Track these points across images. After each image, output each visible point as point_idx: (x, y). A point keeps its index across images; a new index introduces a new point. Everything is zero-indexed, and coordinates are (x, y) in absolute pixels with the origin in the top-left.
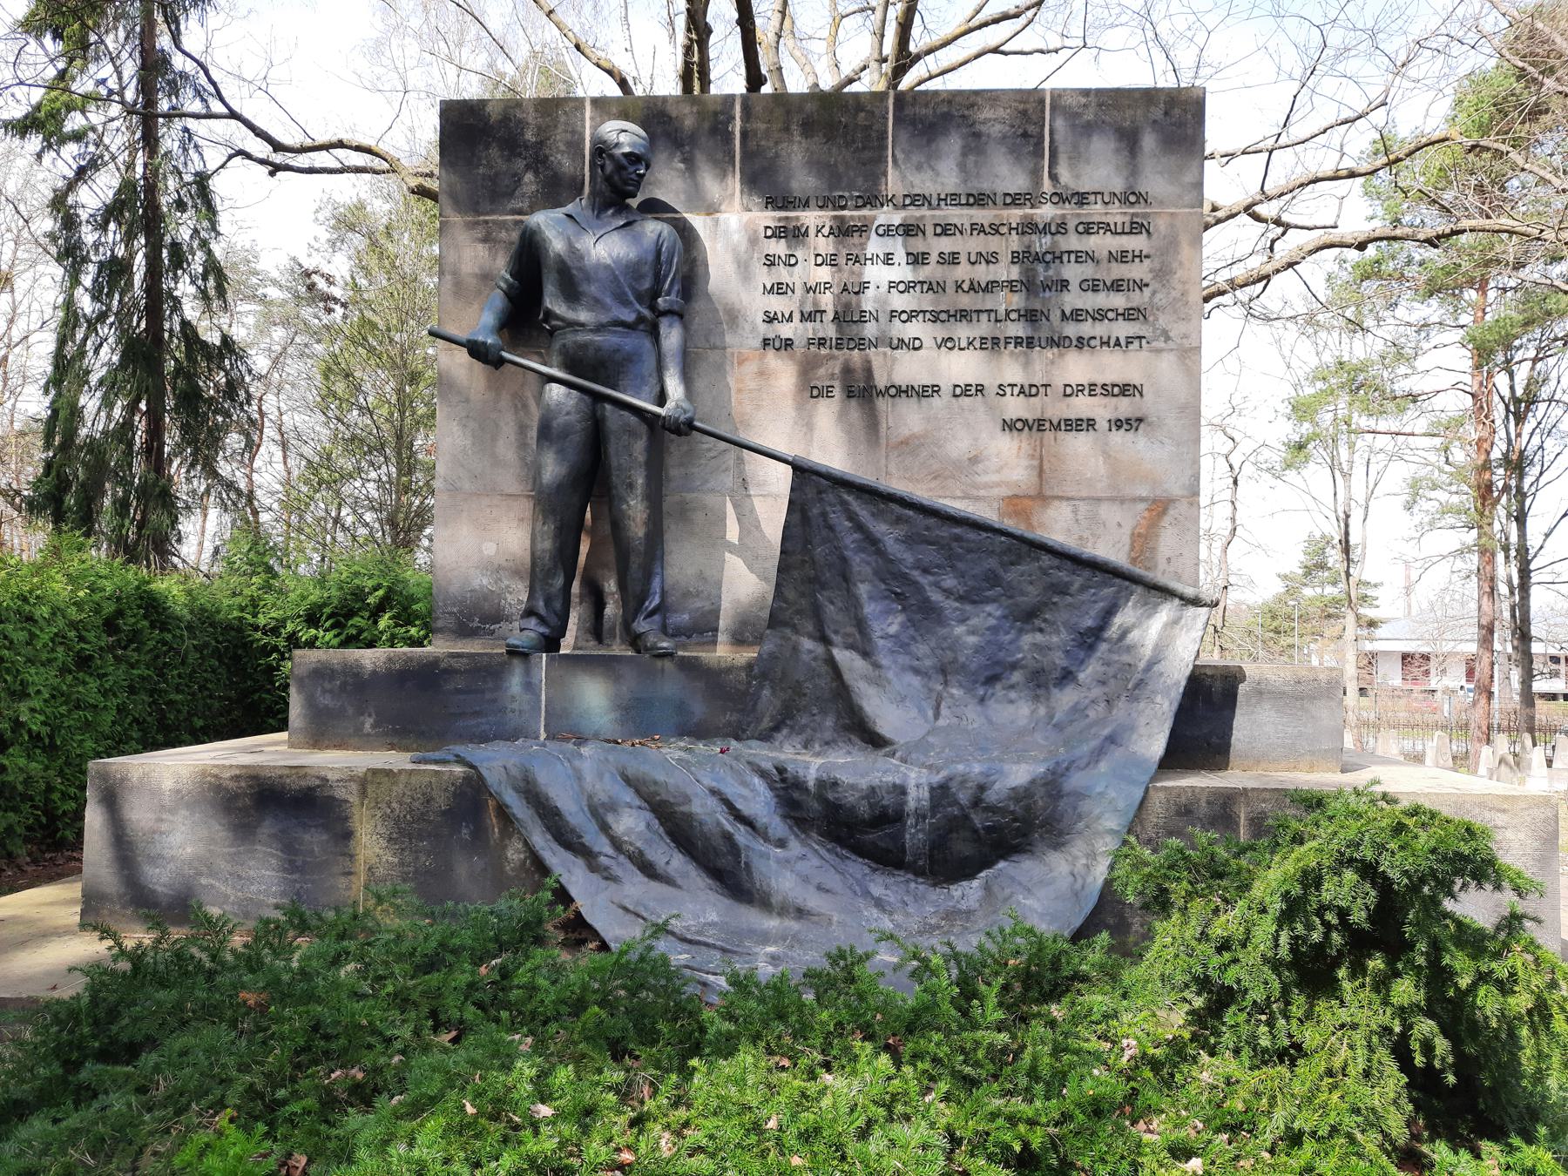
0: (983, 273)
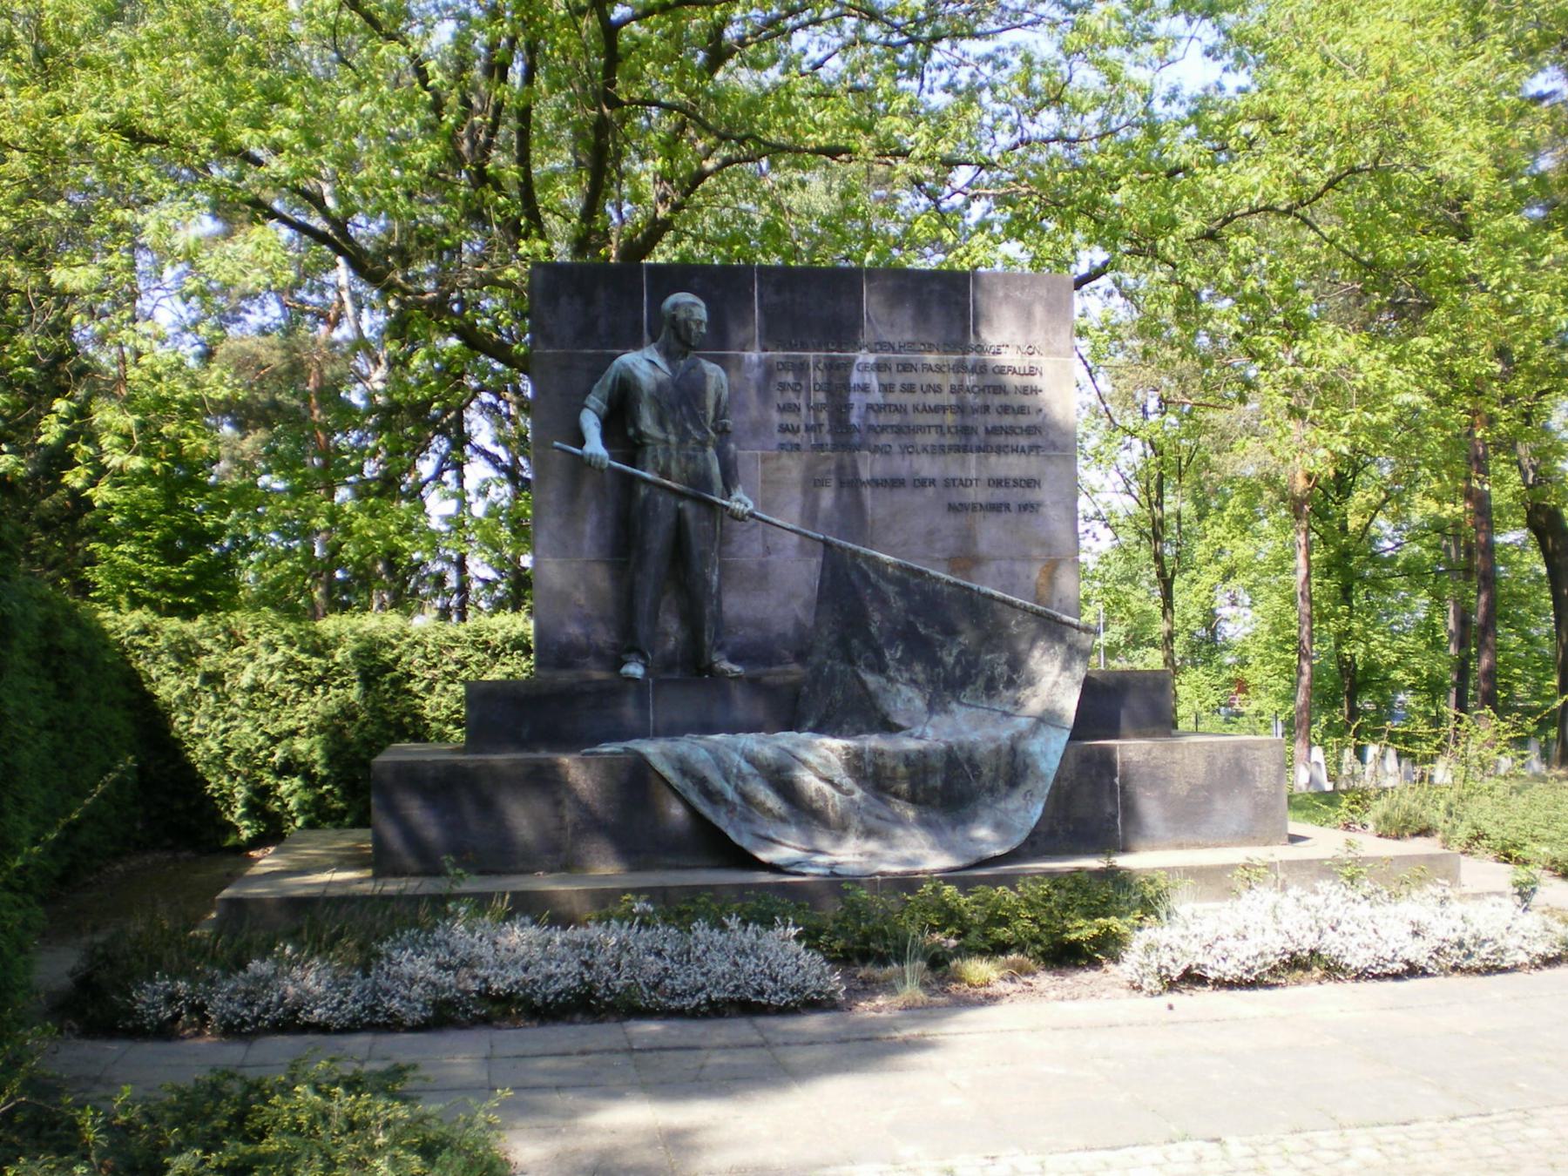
0: (932, 399)
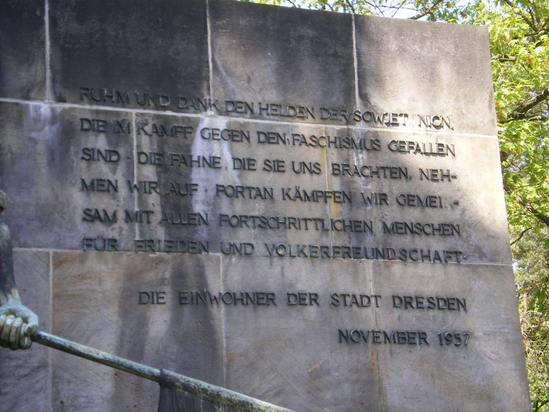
0: (308, 183)
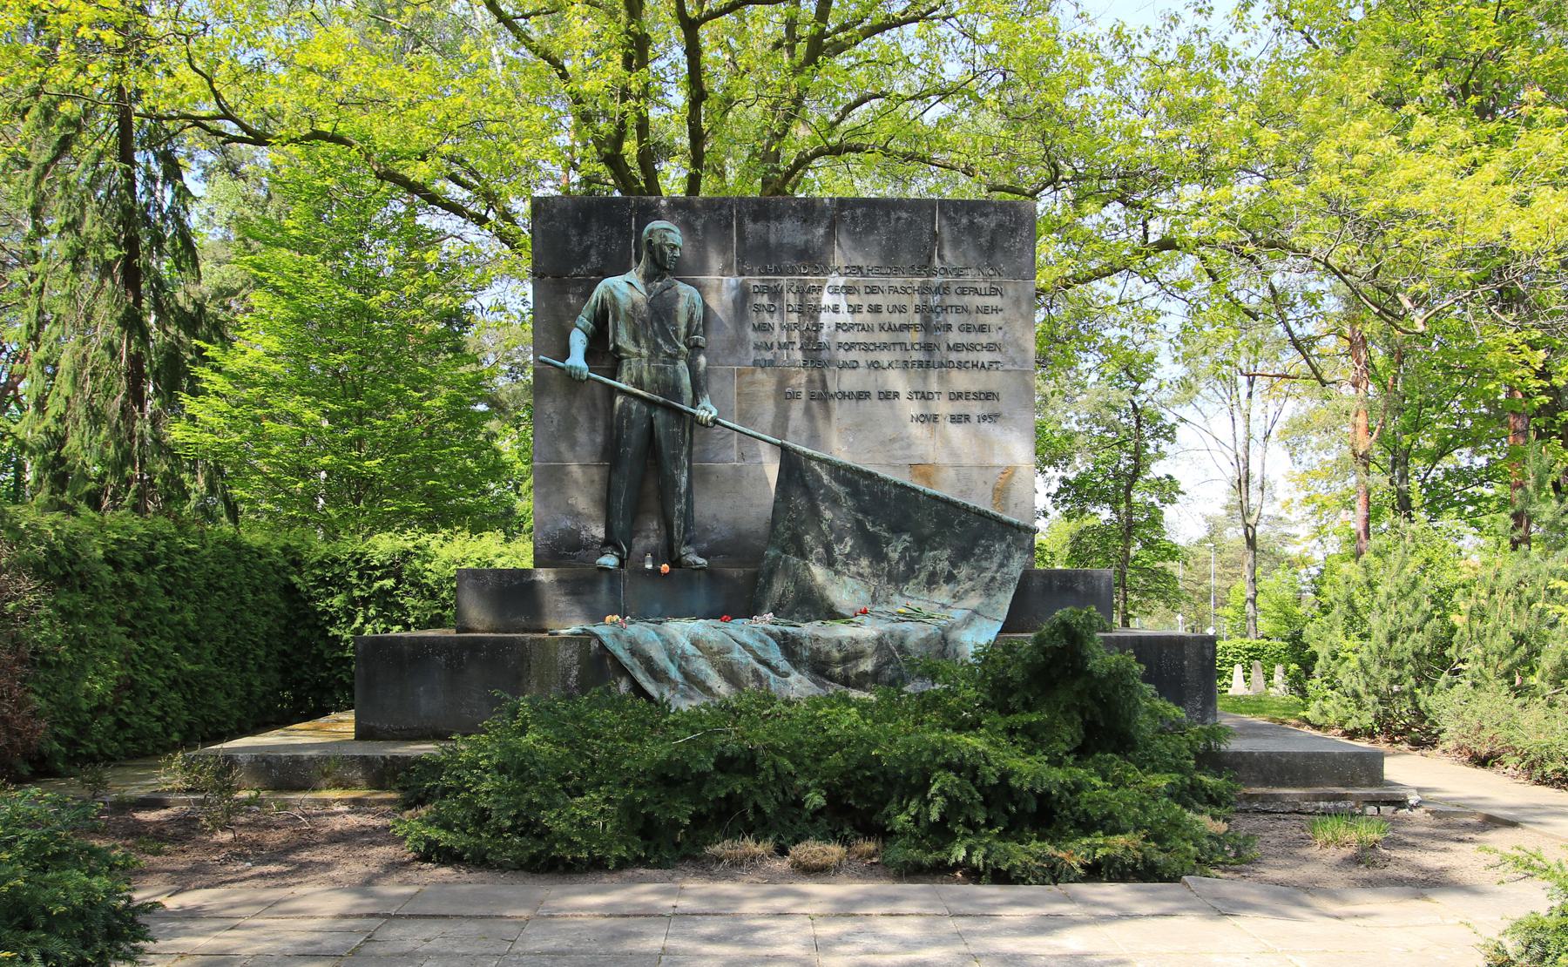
0: (897, 319)
